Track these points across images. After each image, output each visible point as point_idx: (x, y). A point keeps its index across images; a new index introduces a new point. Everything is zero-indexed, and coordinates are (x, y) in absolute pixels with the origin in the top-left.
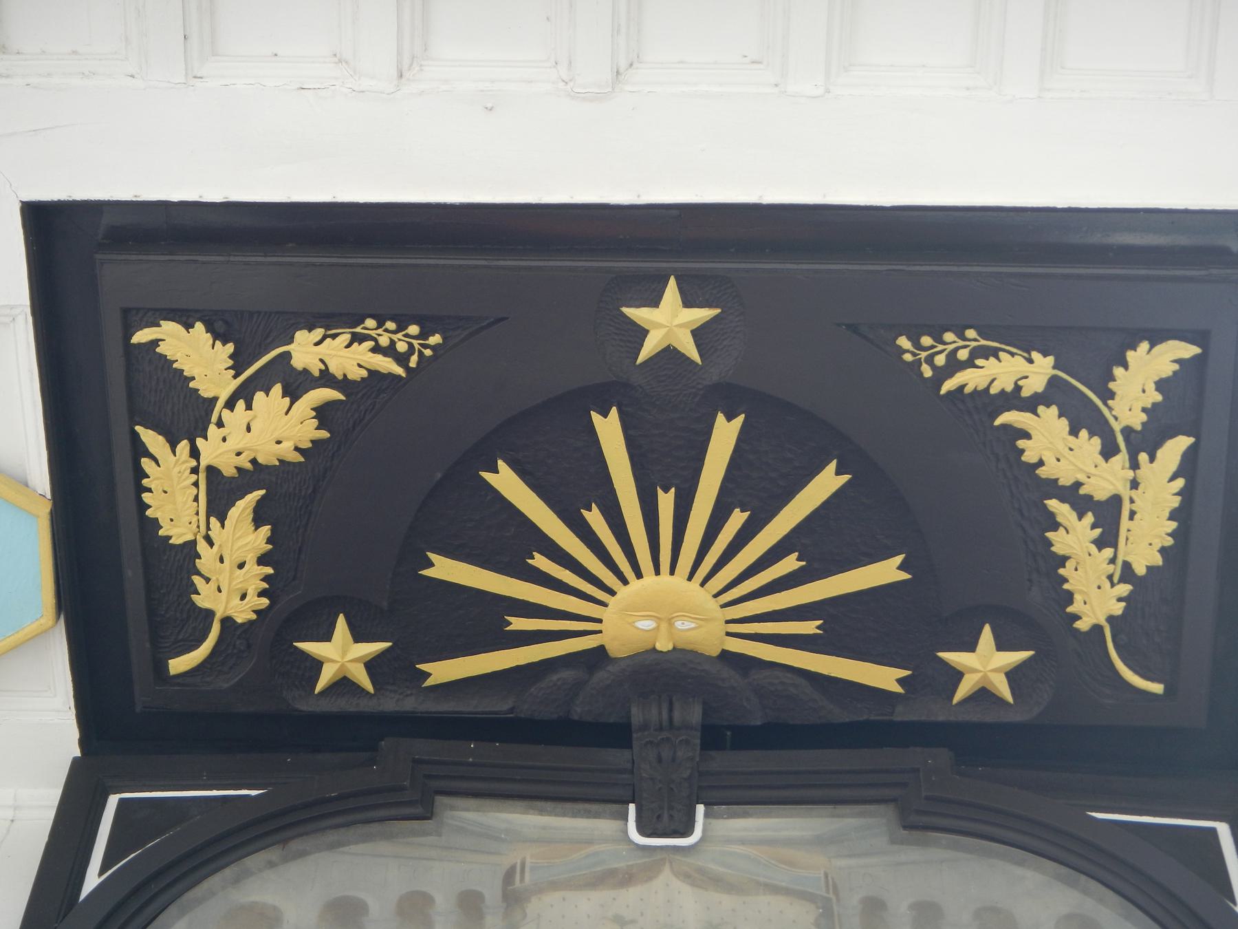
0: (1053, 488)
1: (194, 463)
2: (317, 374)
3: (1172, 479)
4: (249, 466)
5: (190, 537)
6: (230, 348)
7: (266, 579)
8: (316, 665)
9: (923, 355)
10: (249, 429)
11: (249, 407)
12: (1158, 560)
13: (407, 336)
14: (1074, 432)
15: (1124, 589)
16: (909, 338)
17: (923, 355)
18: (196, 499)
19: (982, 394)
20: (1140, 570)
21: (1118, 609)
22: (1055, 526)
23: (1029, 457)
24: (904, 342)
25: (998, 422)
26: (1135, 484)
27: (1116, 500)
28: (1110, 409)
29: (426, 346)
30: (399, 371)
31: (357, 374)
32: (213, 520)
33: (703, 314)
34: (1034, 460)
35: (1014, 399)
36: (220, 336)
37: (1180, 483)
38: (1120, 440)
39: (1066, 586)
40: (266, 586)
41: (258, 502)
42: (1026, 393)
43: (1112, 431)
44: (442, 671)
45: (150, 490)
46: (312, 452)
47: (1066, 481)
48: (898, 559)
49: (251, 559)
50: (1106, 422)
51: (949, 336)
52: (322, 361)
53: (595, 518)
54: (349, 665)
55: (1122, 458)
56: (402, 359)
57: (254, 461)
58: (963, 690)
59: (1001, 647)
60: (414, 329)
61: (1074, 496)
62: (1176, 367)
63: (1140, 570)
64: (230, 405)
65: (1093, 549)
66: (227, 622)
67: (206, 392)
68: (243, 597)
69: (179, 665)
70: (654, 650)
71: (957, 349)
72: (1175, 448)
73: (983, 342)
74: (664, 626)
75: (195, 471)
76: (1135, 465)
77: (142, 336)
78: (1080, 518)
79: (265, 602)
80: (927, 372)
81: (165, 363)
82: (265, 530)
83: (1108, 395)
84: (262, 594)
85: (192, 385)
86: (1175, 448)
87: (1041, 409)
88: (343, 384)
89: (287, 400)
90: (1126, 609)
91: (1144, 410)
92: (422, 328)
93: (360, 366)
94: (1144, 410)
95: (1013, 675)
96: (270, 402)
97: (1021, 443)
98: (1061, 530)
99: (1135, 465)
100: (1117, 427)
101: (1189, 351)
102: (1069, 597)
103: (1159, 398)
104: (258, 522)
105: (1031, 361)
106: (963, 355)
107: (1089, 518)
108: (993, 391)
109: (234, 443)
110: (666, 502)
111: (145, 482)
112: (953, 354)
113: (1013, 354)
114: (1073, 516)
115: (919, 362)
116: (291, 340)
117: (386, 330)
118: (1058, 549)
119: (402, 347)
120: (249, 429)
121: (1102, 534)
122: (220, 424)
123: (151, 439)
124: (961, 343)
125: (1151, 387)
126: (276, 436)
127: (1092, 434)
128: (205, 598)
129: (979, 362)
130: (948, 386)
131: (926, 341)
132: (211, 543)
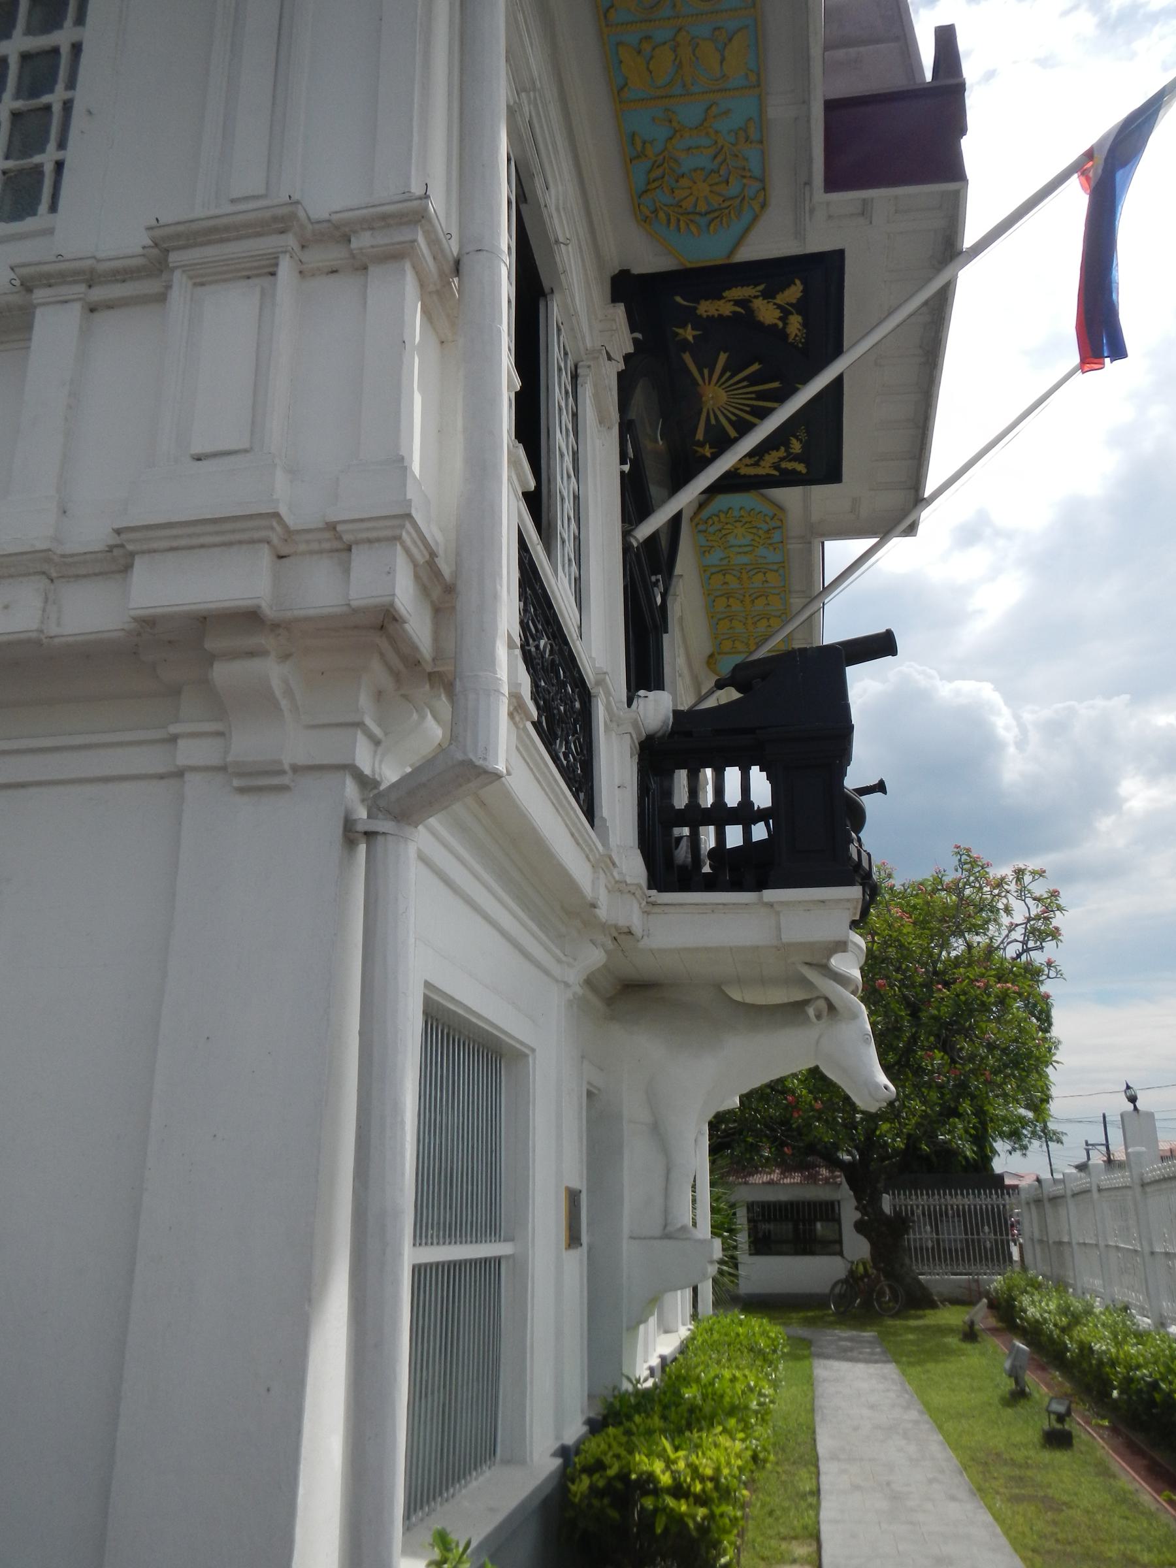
20: (739, 471)
36: (799, 300)
49: (720, 313)
60: (803, 340)
64: (775, 304)
68: (706, 311)
69: (678, 299)
81: (788, 286)
86: (776, 473)
96: (778, 313)
122: (768, 302)
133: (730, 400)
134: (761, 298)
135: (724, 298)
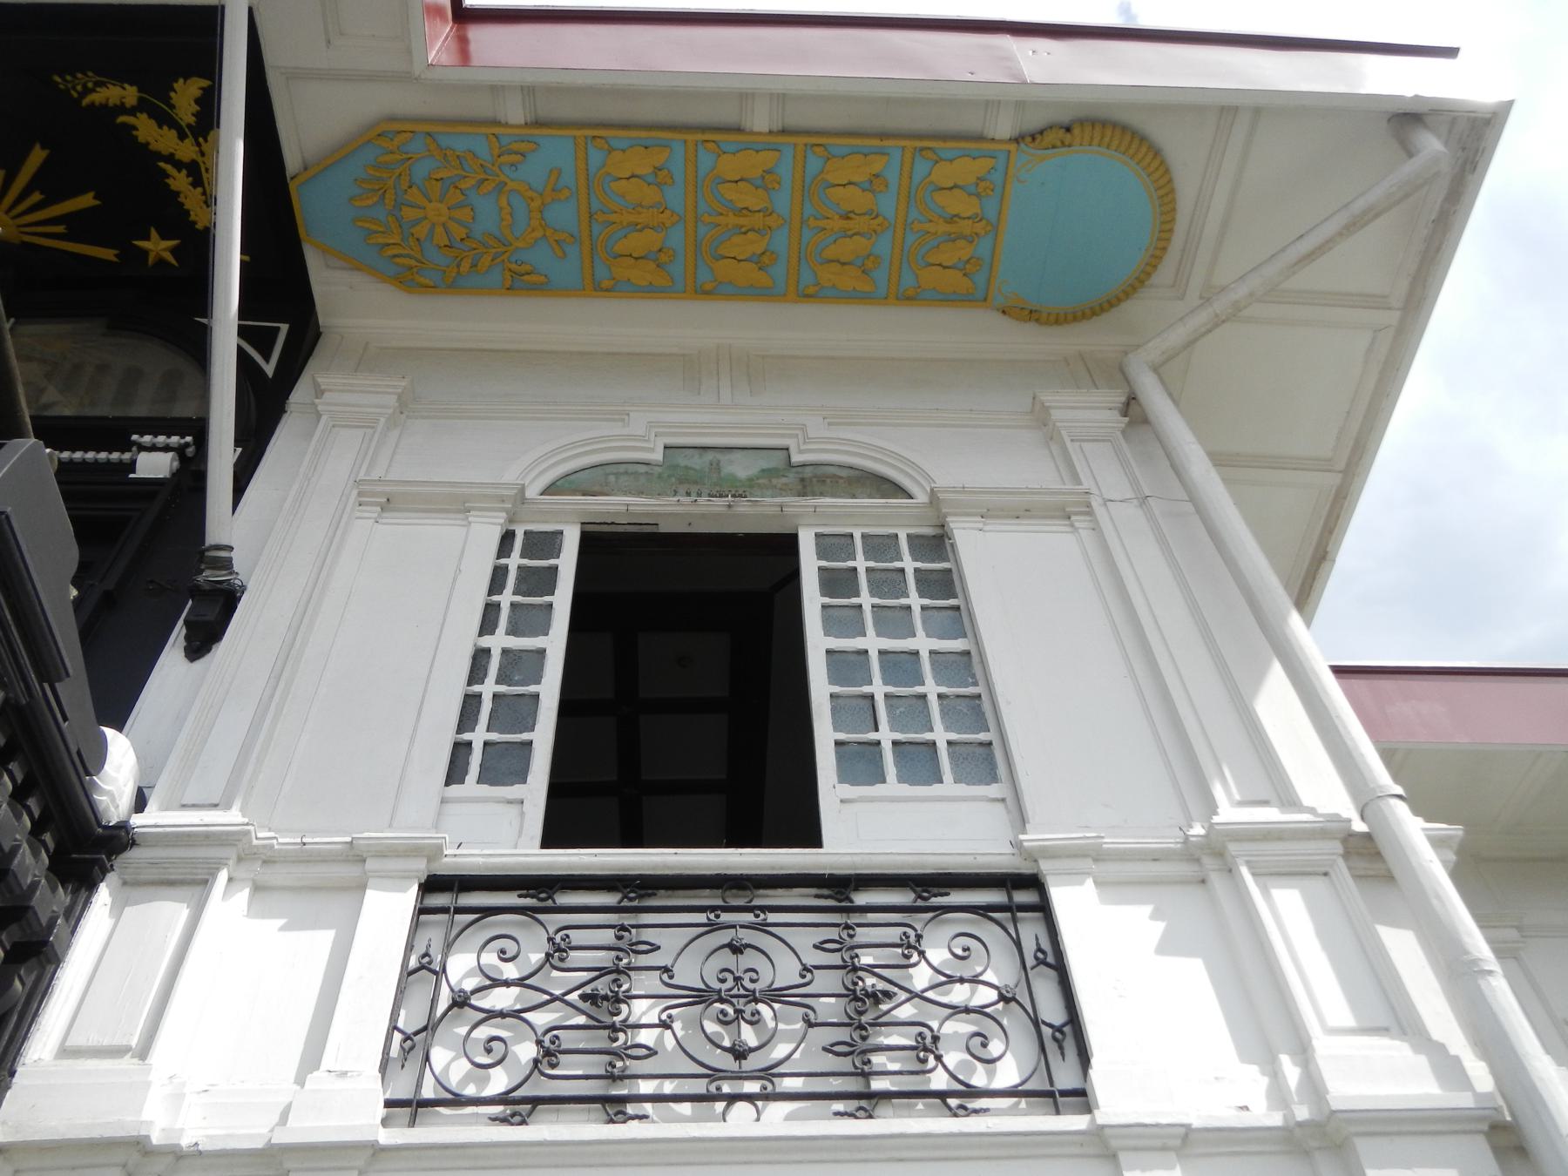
0: (159, 156)
9: (70, 85)
16: (60, 77)
22: (168, 176)
24: (57, 79)
28: (177, 115)
35: (122, 109)
38: (187, 130)
43: (181, 127)
50: (177, 121)
55: (189, 141)
62: (201, 92)
65: (191, 188)
73: (99, 79)
80: (75, 95)
87: (138, 114)
94: (193, 115)
99: (199, 145)
100: (183, 124)
102: (187, 213)
105: (124, 89)
107: (184, 172)
112: (85, 86)
113: (114, 85)
114: (177, 174)
125: (193, 103)
127: (170, 128)
129: (98, 89)
130: (85, 102)
131: (69, 78)
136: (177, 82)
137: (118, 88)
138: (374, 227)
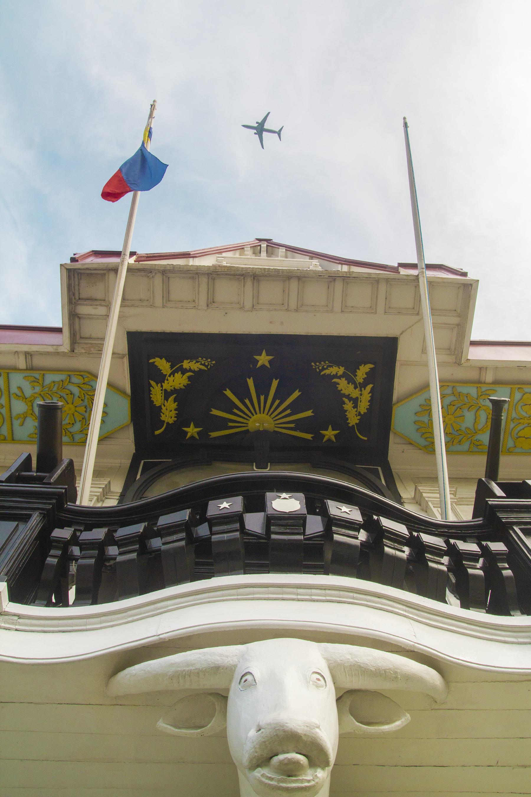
1: (161, 388)
2: (188, 369)
3: (369, 394)
4: (173, 389)
5: (160, 405)
6: (170, 364)
7: (176, 414)
8: (186, 433)
9: (317, 367)
10: (173, 381)
11: (174, 376)
12: (366, 411)
13: (208, 361)
14: (348, 383)
15: (359, 417)
17: (317, 367)
18: (162, 396)
19: (329, 375)
20: (362, 413)
21: (358, 422)
22: (344, 404)
23: (339, 389)
24: (313, 364)
25: (333, 381)
26: (361, 395)
27: (357, 398)
28: (356, 379)
29: (212, 364)
30: (206, 369)
31: (197, 369)
32: (165, 401)
33: (270, 358)
34: (340, 389)
35: (336, 376)
36: (168, 361)
37: (370, 395)
38: (358, 385)
39: (347, 417)
40: (176, 415)
41: (175, 397)
42: (338, 375)
44: (214, 434)
45: (152, 394)
46: (186, 386)
47: (347, 394)
48: (311, 411)
49: (173, 409)
50: (355, 381)
51: (322, 363)
52: (190, 367)
53: (247, 401)
54: (194, 433)
56: (206, 366)
57: (174, 388)
58: (325, 439)
59: (333, 430)
60: (209, 360)
61: (348, 397)
62: (369, 370)
63: (362, 413)
65: (352, 408)
66: (168, 423)
67: (165, 373)
68: (171, 418)
69: (157, 432)
70: (259, 430)
71: (324, 366)
72: (369, 387)
73: (329, 364)
74: (261, 426)
75: (162, 390)
76: (361, 390)
77: (151, 361)
78: (350, 402)
79: (176, 419)
80: (318, 370)
81: (156, 366)
82: (176, 403)
83: (356, 376)
84: (175, 417)
85: (162, 371)
86: (369, 387)
87: (341, 378)
88: (193, 371)
89: (182, 375)
90: (359, 422)
91: (363, 379)
92: (211, 360)
93: (197, 368)
94: (363, 379)
95: (336, 436)
96: (178, 375)
97: (337, 386)
98: (346, 405)
100: (357, 382)
101: (372, 366)
102: (347, 419)
103: (366, 376)
104: (175, 402)
105: (339, 368)
106: (325, 367)
107: (352, 402)
108: (332, 374)
109: (170, 384)
110: (262, 398)
111: (151, 392)
112: (323, 367)
113: (336, 367)
114: (348, 402)
115: (316, 368)
116: (183, 362)
117: (204, 360)
118: (345, 409)
119: (206, 364)
120: (173, 381)
121: (354, 405)
122: (167, 380)
123: (152, 383)
124: (325, 364)
125: (364, 374)
126: (179, 383)
128: (163, 418)
129: (329, 368)
130: (322, 373)
131: (318, 364)
132: (165, 406)
133: (250, 414)
134: (163, 384)
135: (161, 406)
136: (361, 366)
137: (337, 368)
138: (423, 425)
